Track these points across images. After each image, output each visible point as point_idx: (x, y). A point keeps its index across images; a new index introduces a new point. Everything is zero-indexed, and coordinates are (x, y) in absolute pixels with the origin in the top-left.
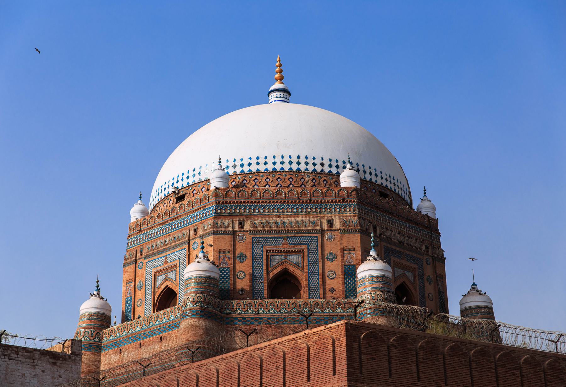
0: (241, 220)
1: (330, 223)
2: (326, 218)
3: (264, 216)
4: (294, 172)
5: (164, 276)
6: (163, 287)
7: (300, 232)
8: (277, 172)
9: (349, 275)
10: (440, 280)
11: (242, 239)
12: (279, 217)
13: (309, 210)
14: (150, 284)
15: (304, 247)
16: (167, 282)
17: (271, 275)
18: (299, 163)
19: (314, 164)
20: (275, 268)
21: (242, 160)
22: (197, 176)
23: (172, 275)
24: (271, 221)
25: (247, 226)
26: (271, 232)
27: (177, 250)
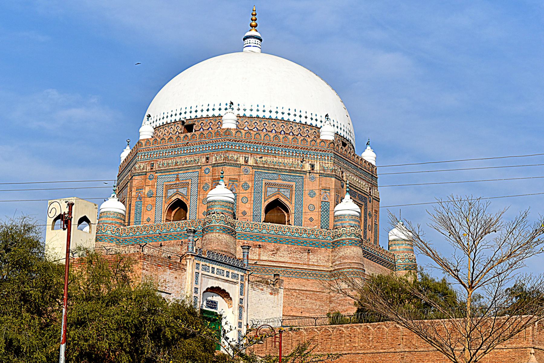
0: (247, 156)
1: (313, 166)
5: (175, 190)
6: (173, 198)
12: (276, 157)
15: (294, 184)
17: (267, 203)
22: (205, 111)
25: (251, 162)
27: (190, 171)
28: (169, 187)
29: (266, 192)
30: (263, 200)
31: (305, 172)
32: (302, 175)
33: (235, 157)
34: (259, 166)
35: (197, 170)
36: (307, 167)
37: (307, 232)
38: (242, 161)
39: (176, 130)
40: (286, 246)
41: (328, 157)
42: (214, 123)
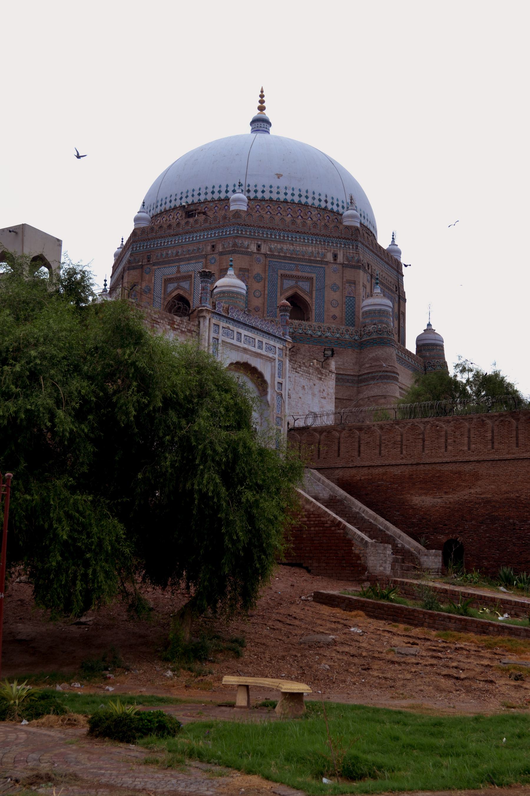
0: (259, 243)
1: (335, 256)
2: (332, 251)
3: (279, 242)
4: (302, 204)
5: (176, 285)
6: (174, 294)
7: (310, 261)
8: (288, 202)
9: (349, 305)
10: (400, 316)
11: (260, 261)
12: (293, 245)
13: (318, 242)
14: (159, 289)
15: (314, 276)
16: (179, 290)
18: (307, 197)
19: (320, 200)
20: (287, 290)
21: (256, 186)
23: (185, 285)
24: (285, 247)
25: (264, 249)
26: (285, 258)
28: (168, 281)
29: (282, 284)
30: (279, 294)
31: (327, 263)
32: (323, 266)
33: (246, 243)
34: (274, 255)
35: (201, 260)
36: (330, 257)
37: (332, 331)
38: (253, 248)
39: (176, 217)
40: (307, 346)
41: (353, 246)
42: (220, 206)
